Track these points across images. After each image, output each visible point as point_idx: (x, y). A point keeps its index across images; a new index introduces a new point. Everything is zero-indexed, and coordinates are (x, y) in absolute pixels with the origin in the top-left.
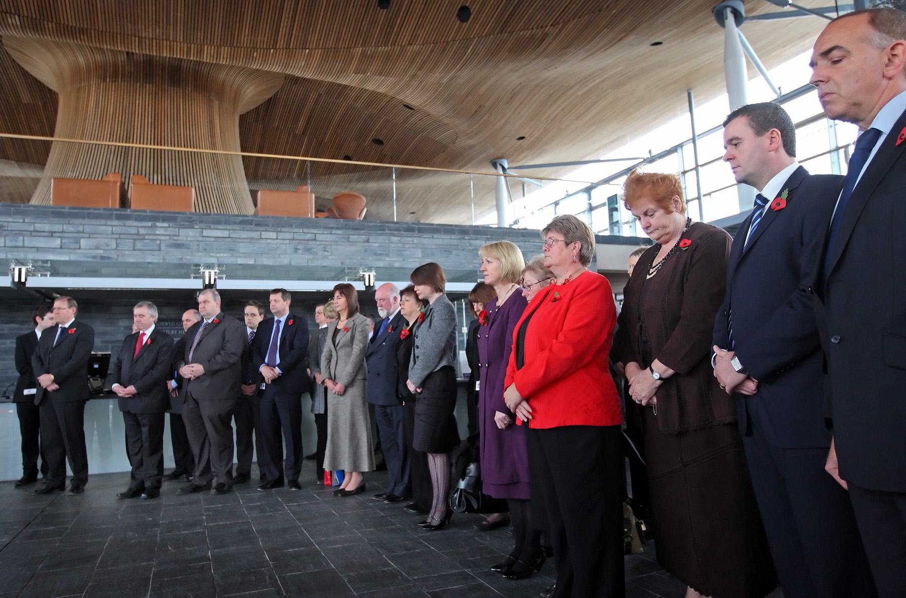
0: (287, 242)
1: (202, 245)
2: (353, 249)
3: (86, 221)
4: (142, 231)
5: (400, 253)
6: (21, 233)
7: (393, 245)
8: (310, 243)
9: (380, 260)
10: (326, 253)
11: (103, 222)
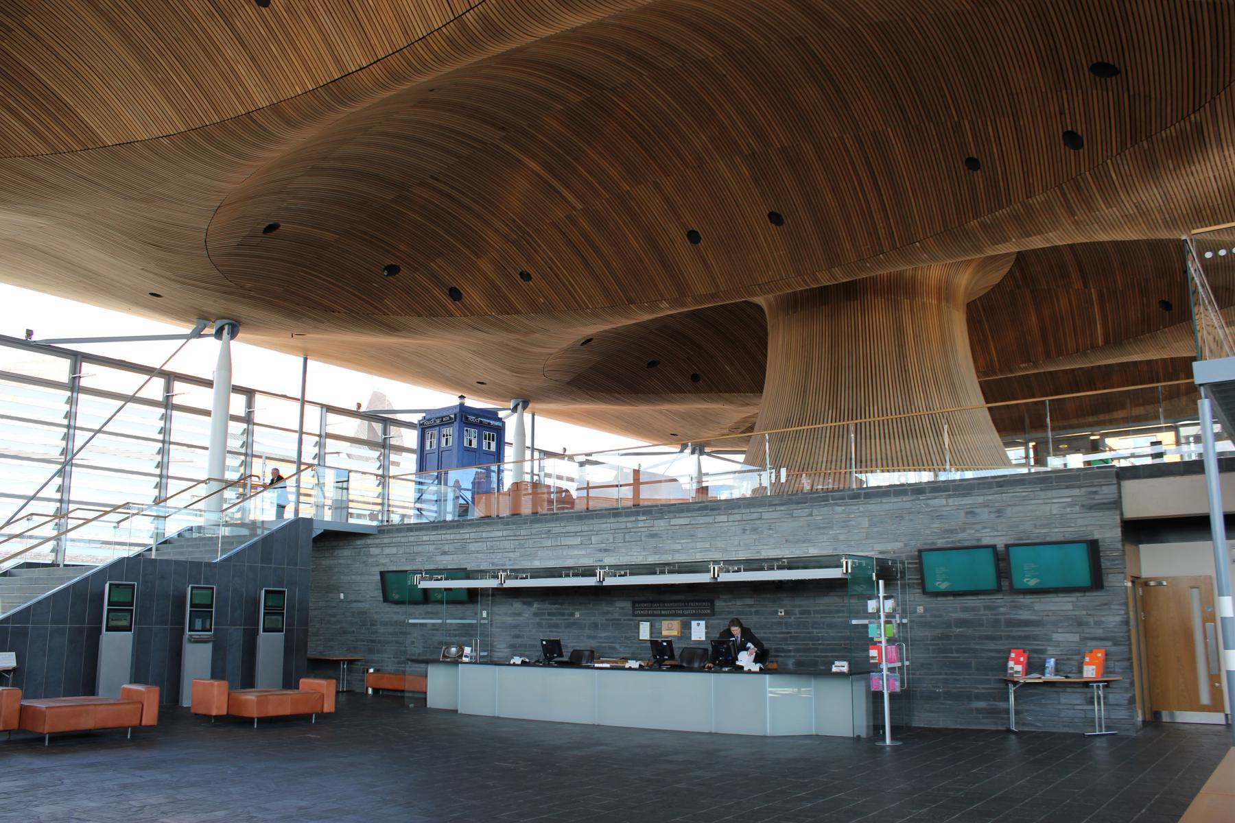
3: (595, 521)
4: (629, 525)
6: (559, 535)
11: (604, 520)
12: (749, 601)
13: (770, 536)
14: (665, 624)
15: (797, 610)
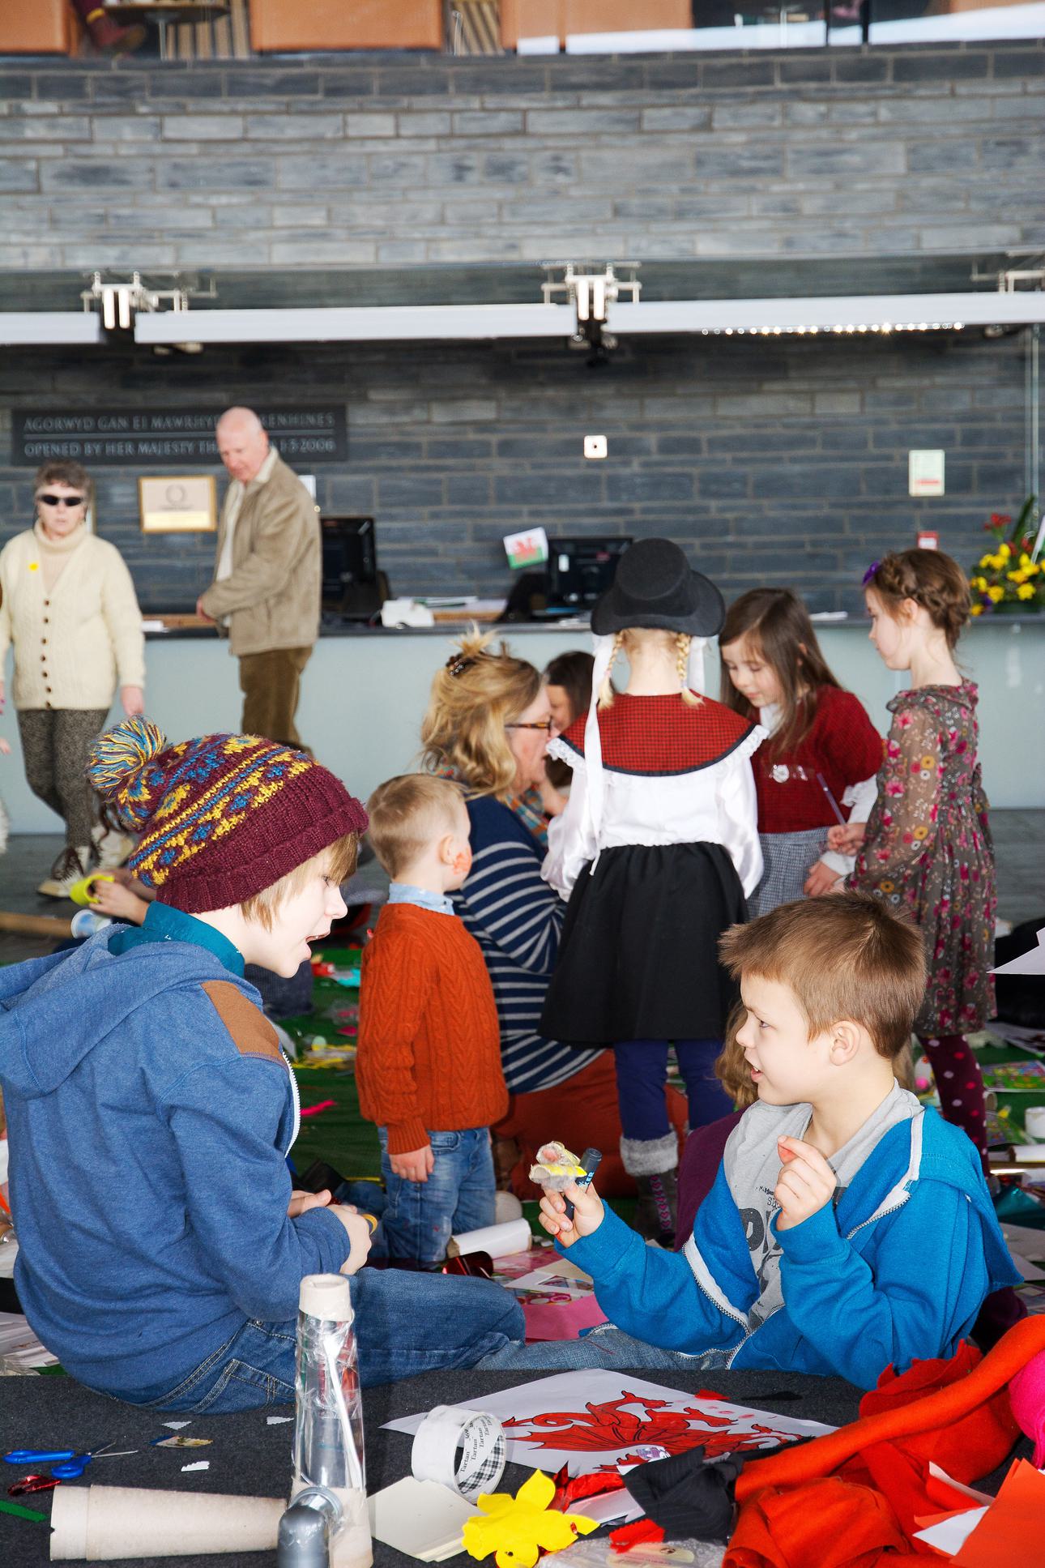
0: (431, 145)
1: (162, 167)
2: (654, 157)
5: (824, 162)
7: (799, 135)
8: (508, 144)
9: (752, 190)
10: (561, 179)
12: (481, 411)
13: (555, 193)
14: (154, 490)
15: (652, 439)
